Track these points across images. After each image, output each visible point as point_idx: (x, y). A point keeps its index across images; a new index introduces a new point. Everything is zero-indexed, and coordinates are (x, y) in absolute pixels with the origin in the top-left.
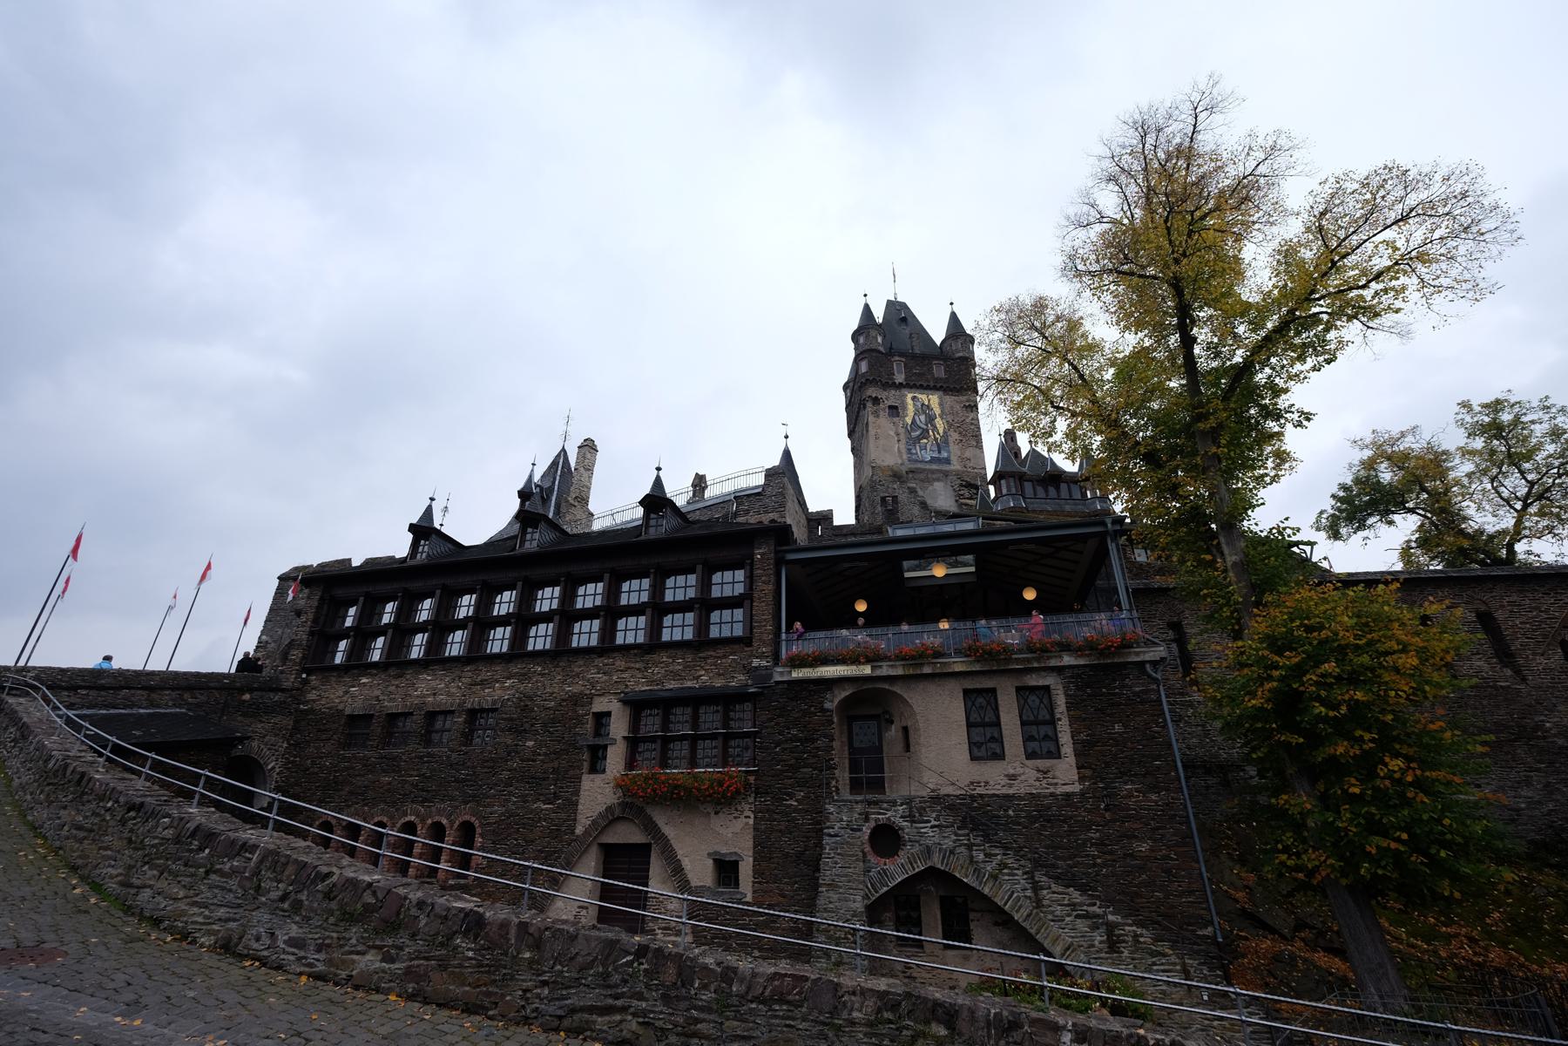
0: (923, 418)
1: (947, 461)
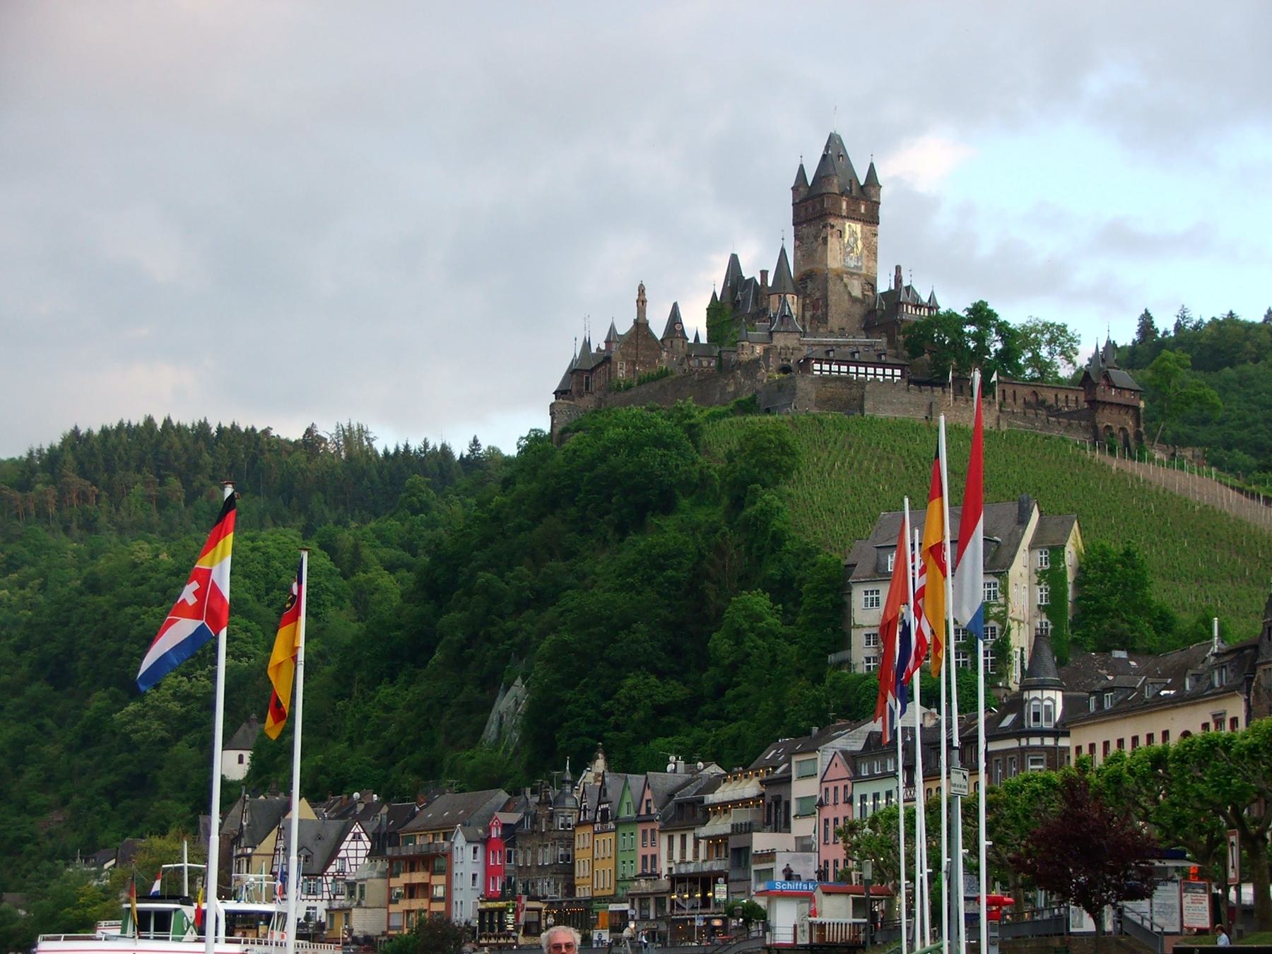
0: (852, 239)
1: (860, 268)
